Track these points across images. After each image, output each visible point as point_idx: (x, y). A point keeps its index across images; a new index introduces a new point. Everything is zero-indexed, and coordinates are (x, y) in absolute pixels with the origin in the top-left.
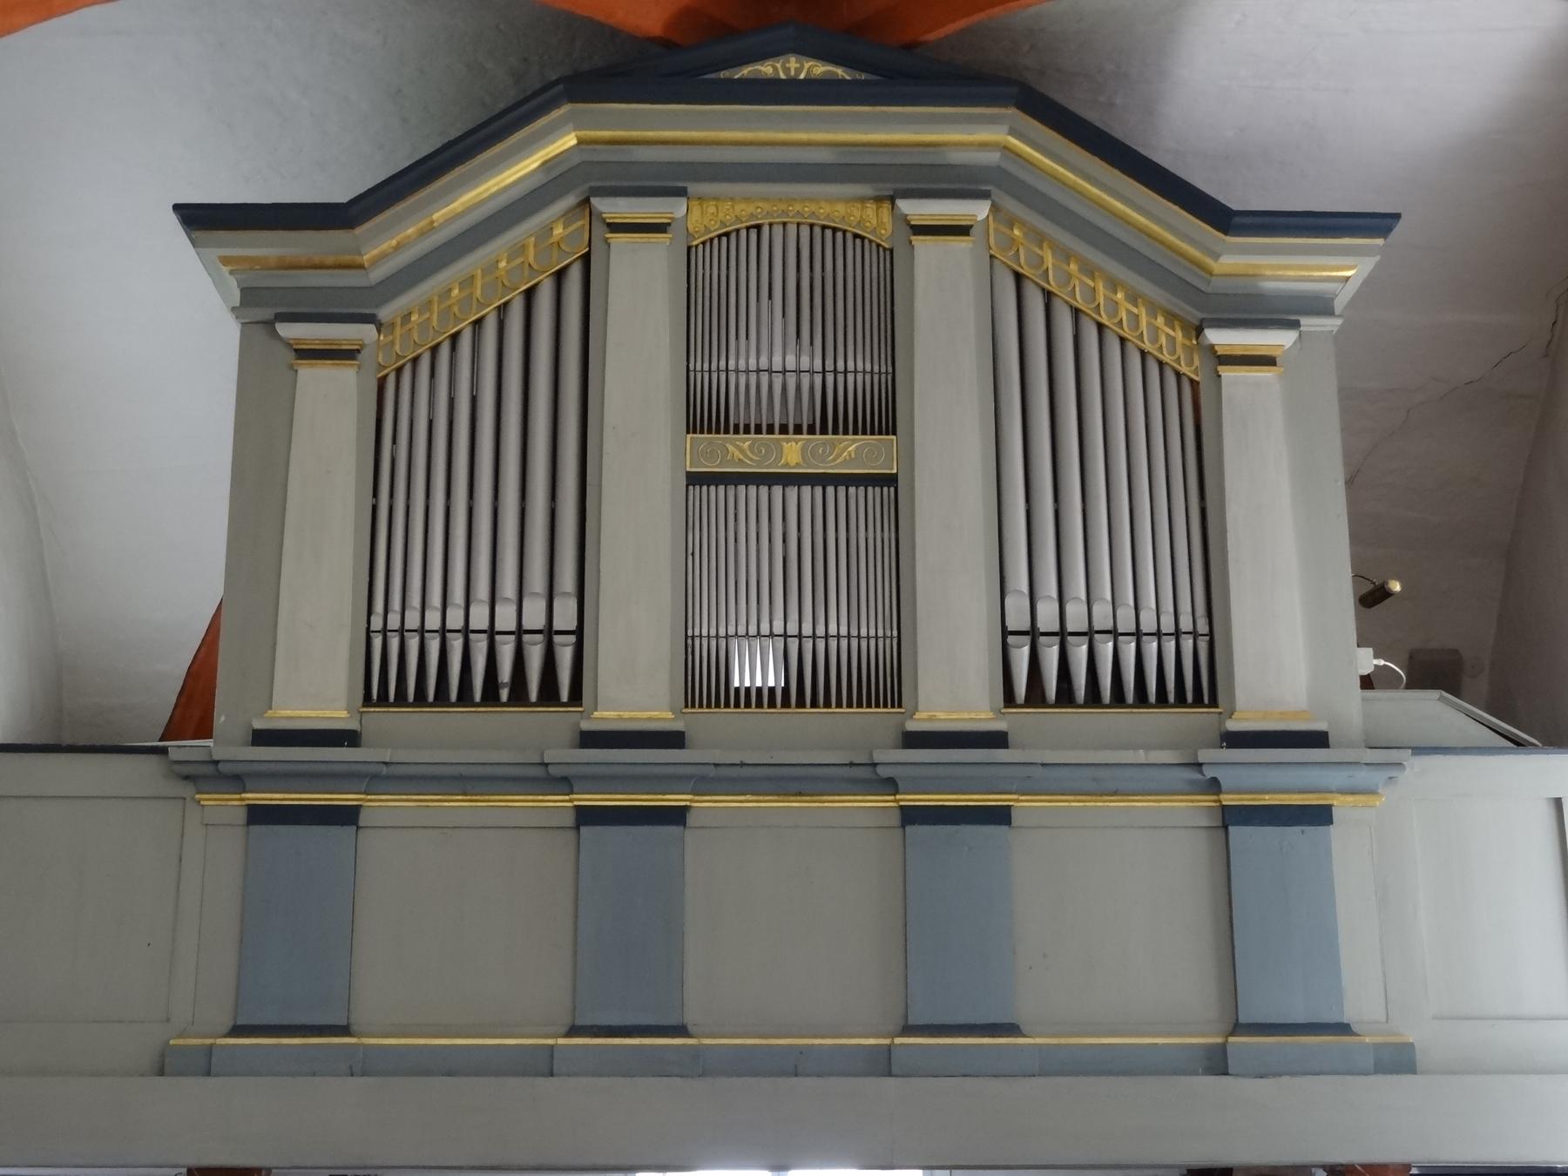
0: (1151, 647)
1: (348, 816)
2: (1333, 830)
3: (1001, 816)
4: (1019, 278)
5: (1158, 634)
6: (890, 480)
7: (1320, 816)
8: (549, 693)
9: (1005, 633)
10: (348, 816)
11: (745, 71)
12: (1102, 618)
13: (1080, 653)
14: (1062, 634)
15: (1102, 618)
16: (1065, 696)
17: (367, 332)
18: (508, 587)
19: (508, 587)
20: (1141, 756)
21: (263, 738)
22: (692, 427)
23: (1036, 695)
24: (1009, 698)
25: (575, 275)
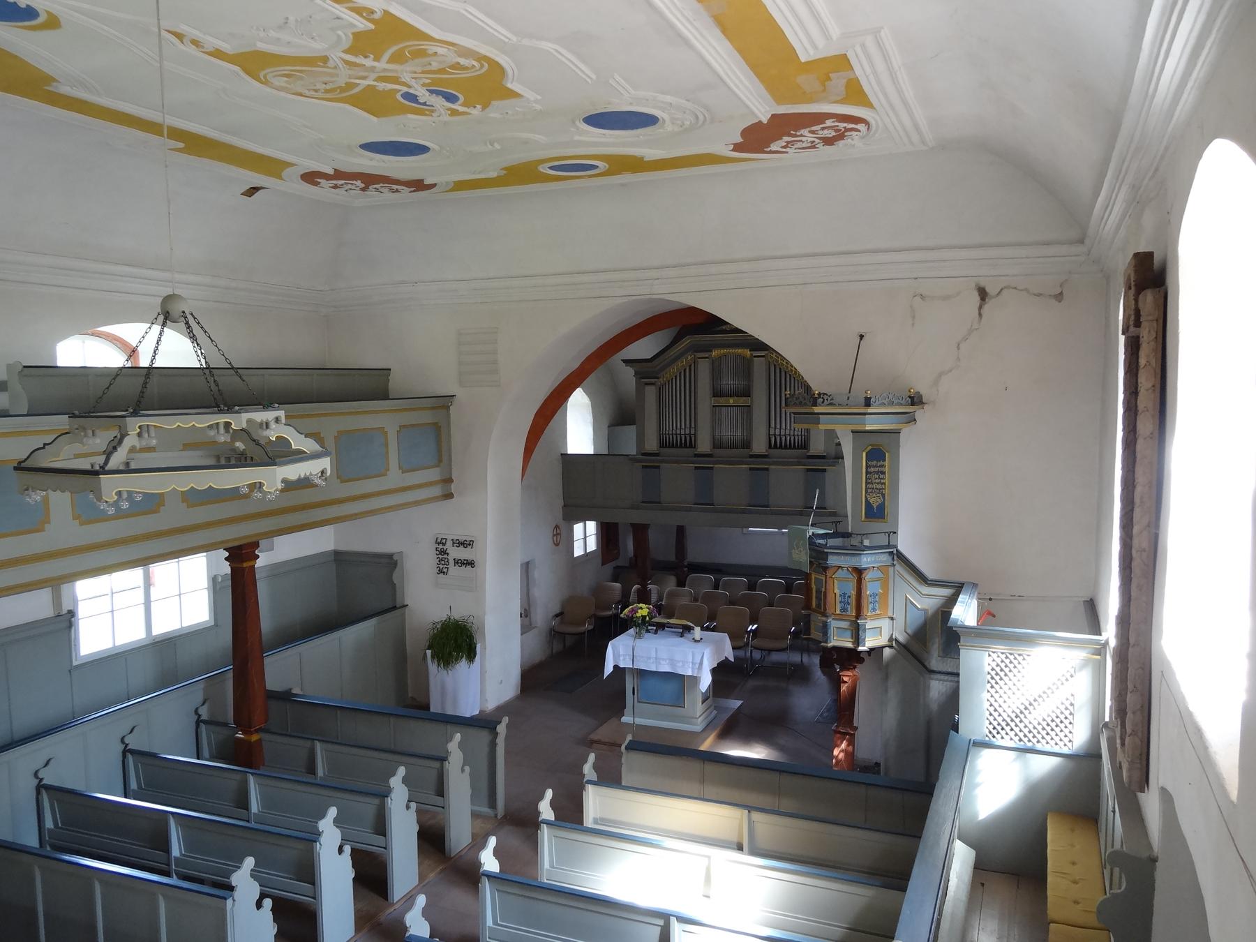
0: (797, 438)
1: (658, 467)
2: (826, 473)
3: (767, 469)
4: (775, 366)
5: (798, 435)
6: (749, 406)
7: (824, 470)
8: (691, 446)
9: (769, 435)
10: (658, 467)
11: (718, 329)
12: (787, 433)
13: (783, 439)
14: (780, 435)
15: (787, 433)
16: (781, 447)
17: (656, 380)
18: (683, 427)
19: (683, 427)
20: (792, 460)
21: (644, 454)
22: (714, 396)
23: (775, 447)
24: (770, 447)
25: (693, 365)
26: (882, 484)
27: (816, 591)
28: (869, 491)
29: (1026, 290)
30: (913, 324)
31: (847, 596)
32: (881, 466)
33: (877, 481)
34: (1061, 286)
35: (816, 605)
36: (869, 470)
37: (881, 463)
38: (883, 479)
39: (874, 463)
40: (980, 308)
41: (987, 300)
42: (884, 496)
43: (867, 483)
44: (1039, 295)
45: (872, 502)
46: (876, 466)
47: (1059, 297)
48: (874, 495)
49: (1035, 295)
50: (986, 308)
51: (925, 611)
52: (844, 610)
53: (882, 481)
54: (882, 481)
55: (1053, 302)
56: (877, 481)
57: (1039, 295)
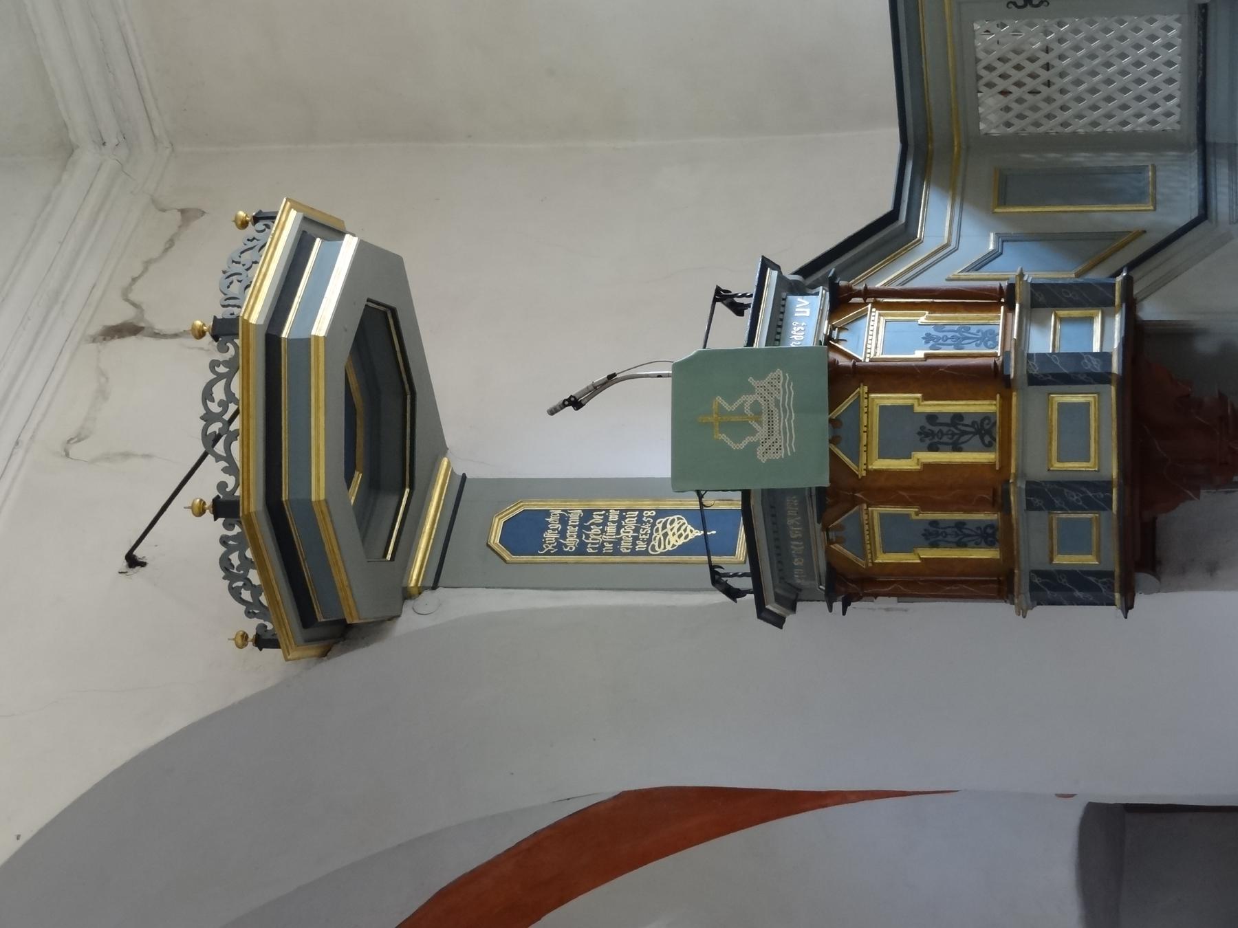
26: (622, 517)
27: (933, 448)
28: (641, 546)
29: (147, 264)
30: (147, 456)
31: (933, 332)
32: (564, 520)
33: (611, 529)
34: (164, 210)
35: (988, 447)
36: (571, 542)
37: (554, 521)
38: (606, 518)
39: (550, 536)
40: (157, 335)
41: (142, 325)
42: (661, 513)
43: (616, 552)
44: (171, 243)
45: (682, 541)
46: (563, 534)
47: (188, 215)
48: (659, 535)
49: (166, 250)
50: (160, 326)
51: (1002, 239)
52: (988, 338)
53: (614, 516)
54: (614, 516)
55: (196, 224)
56: (611, 529)
57: (171, 243)
